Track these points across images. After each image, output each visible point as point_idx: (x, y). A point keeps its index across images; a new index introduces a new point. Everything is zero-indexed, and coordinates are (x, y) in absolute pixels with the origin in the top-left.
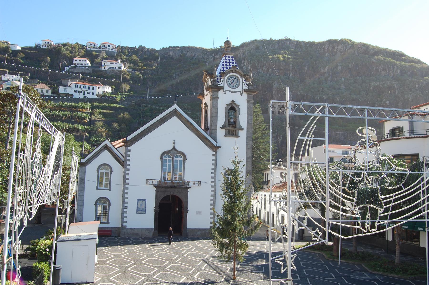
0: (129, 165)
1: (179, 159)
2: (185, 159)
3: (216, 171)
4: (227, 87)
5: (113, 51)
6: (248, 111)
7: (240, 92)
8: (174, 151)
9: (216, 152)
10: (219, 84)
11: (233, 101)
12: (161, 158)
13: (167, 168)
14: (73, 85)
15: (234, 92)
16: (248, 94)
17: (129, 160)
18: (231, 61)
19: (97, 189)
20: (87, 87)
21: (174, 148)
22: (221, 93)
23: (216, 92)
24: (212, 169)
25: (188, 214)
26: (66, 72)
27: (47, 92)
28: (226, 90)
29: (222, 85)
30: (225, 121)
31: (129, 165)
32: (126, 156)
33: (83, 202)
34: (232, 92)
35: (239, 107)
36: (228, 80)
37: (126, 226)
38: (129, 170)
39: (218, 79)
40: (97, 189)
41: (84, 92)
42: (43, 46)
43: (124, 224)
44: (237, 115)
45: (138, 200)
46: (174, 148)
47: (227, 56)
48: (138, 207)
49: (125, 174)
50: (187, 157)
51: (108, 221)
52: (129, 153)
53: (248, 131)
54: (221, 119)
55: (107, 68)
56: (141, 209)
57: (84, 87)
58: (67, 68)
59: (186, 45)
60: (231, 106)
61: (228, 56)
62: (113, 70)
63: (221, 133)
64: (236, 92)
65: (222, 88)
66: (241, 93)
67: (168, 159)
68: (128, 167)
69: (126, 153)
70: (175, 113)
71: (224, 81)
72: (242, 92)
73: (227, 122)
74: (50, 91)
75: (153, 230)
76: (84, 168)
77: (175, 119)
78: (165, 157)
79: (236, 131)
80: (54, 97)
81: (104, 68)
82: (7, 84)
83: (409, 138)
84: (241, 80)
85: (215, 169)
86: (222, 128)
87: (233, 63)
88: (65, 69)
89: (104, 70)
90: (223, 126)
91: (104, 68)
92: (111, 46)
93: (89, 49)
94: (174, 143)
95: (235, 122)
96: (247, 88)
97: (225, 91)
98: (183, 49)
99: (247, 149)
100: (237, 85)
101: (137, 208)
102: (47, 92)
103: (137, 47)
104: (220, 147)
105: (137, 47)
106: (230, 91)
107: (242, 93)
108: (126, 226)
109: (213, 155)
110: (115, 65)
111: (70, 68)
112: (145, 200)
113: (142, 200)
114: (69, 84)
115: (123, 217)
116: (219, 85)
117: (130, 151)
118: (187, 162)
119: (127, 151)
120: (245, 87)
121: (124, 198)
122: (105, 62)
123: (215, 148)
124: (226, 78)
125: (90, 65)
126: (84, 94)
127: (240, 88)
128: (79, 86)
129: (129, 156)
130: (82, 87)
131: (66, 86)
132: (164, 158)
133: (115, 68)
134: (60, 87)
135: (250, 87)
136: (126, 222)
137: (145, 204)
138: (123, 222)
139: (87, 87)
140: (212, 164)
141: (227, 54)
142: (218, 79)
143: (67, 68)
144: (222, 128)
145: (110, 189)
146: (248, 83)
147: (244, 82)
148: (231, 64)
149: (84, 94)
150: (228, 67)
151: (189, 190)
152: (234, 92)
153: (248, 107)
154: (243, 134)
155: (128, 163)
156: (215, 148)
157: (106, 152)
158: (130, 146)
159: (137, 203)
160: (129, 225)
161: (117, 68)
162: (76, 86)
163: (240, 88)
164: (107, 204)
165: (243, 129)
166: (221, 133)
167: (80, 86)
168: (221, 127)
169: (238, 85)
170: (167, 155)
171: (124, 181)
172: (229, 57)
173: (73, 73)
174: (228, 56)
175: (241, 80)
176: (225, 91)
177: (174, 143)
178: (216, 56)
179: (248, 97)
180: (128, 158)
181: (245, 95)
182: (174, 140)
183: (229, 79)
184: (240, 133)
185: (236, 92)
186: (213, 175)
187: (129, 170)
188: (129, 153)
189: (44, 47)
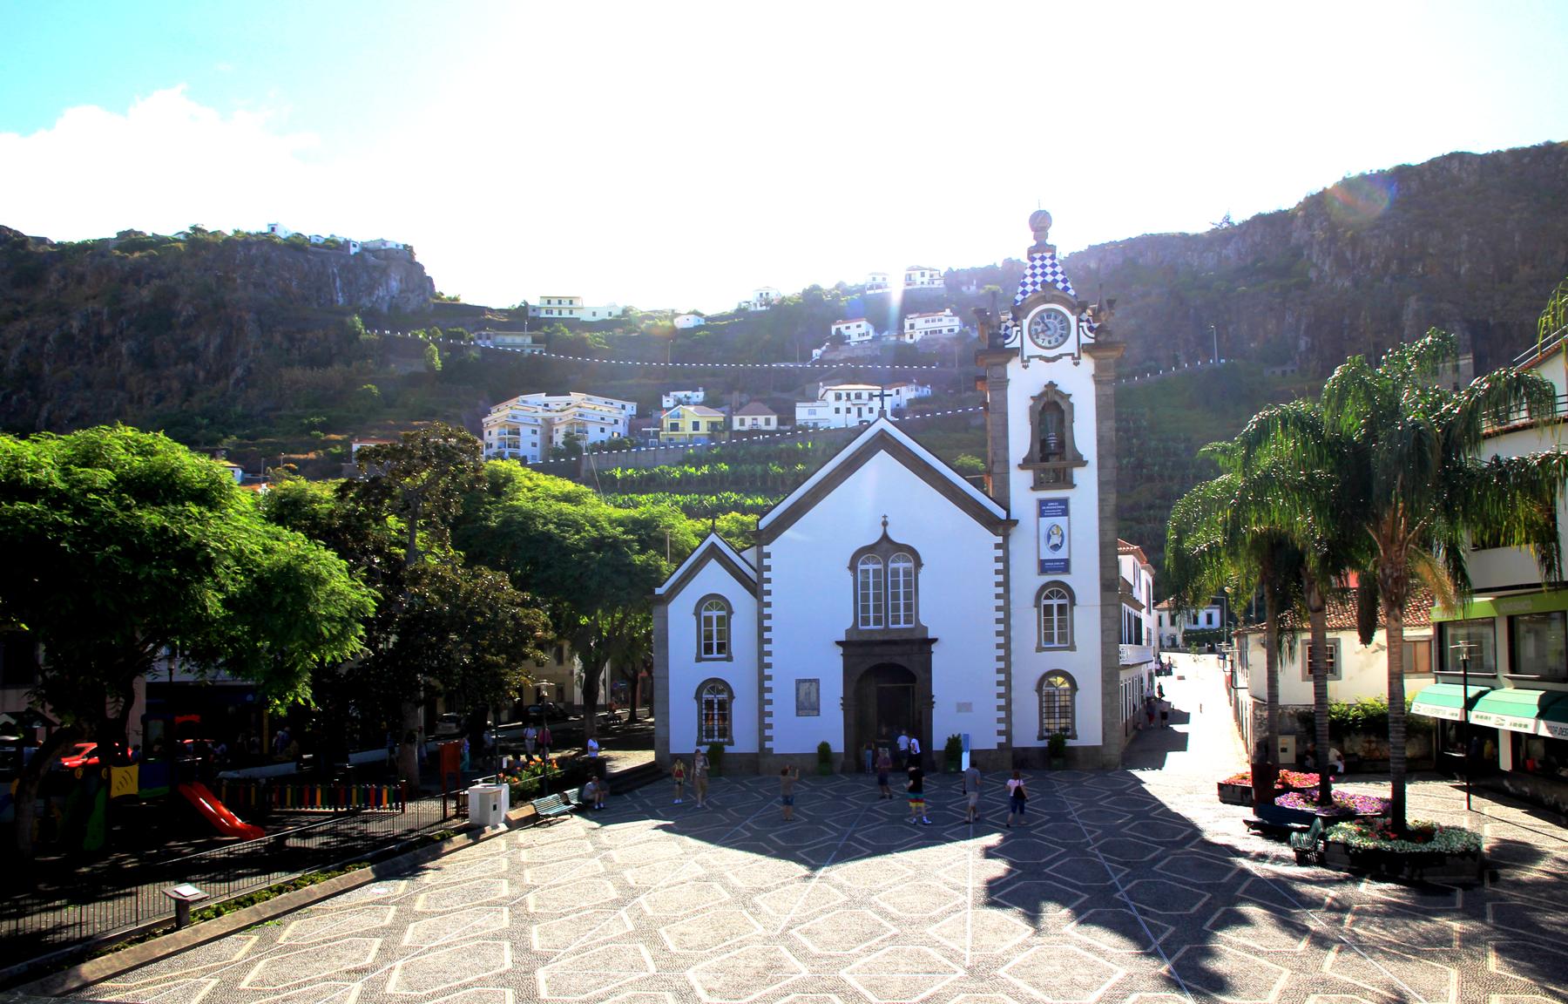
0: (769, 593)
1: (901, 566)
2: (918, 564)
3: (1007, 590)
4: (1030, 349)
5: (932, 286)
6: (1098, 408)
7: (1072, 354)
8: (885, 545)
9: (1006, 537)
10: (1007, 341)
11: (1051, 386)
12: (853, 567)
13: (871, 591)
14: (831, 396)
15: (1054, 359)
16: (1094, 358)
17: (769, 581)
18: (1049, 270)
19: (699, 659)
20: (865, 396)
21: (885, 537)
22: (1013, 368)
23: (999, 367)
24: (998, 584)
25: (936, 714)
26: (813, 364)
27: (768, 422)
28: (1029, 357)
29: (1017, 344)
30: (1032, 445)
31: (769, 593)
32: (760, 569)
33: (668, 694)
34: (1048, 360)
35: (1072, 400)
36: (1033, 327)
37: (771, 749)
38: (769, 605)
39: (1007, 328)
40: (699, 659)
41: (860, 410)
42: (755, 305)
43: (768, 745)
44: (1067, 423)
45: (799, 682)
46: (885, 537)
47: (1037, 255)
48: (801, 698)
49: (762, 617)
50: (924, 561)
51: (731, 737)
52: (766, 562)
53: (1101, 467)
54: (1020, 440)
55: (918, 336)
56: (806, 704)
57: (858, 396)
58: (817, 353)
59: (1135, 232)
60: (1045, 399)
61: (1039, 255)
62: (933, 340)
63: (1020, 483)
64: (1060, 356)
65: (1016, 352)
66: (1073, 358)
67: (871, 567)
68: (766, 599)
69: (760, 561)
70: (884, 441)
71: (1021, 331)
72: (1076, 355)
73: (1038, 447)
74: (774, 419)
75: (843, 758)
76: (662, 608)
77: (882, 457)
78: (863, 563)
79: (1065, 469)
80: (783, 433)
81: (911, 337)
82: (672, 416)
83: (1497, 434)
84: (1073, 319)
85: (1006, 584)
86: (1021, 467)
87: (1054, 274)
88: (814, 355)
89: (911, 341)
90: (1025, 460)
91: (911, 337)
92: (927, 273)
93: (871, 292)
94: (885, 524)
95: (1061, 444)
96: (1092, 341)
97: (1025, 358)
98: (1131, 243)
99: (1102, 519)
100: (1061, 336)
101: (797, 700)
102: (768, 422)
103: (999, 265)
104: (1016, 522)
105: (999, 265)
106: (1041, 358)
107: (1079, 358)
108: (771, 749)
109: (998, 546)
110: (939, 324)
111: (824, 352)
112: (817, 681)
113: (810, 680)
114: (821, 391)
115: (763, 726)
116: (1007, 346)
117: (768, 555)
118: (923, 571)
119: (763, 556)
120: (1084, 340)
121: (762, 678)
122: (912, 321)
123: (1002, 526)
124: (1026, 322)
125: (872, 333)
126: (860, 415)
127: (1070, 346)
128: (844, 397)
129: (768, 568)
130: (853, 396)
131: (814, 400)
132: (861, 567)
133: (940, 331)
134: (798, 404)
135: (1102, 338)
136: (770, 738)
137: (818, 690)
138: (763, 739)
139: (865, 396)
140: (997, 572)
141: (1037, 252)
142: (1007, 328)
143: (817, 353)
144: (1021, 467)
145: (729, 658)
146: (1096, 325)
147: (1081, 324)
148: (1039, 279)
149: (860, 415)
150: (1029, 288)
151: (934, 647)
152: (1054, 359)
153: (1097, 396)
154: (1087, 480)
155: (766, 587)
156: (1002, 526)
157: (713, 564)
158: (767, 544)
159: (797, 690)
160: (779, 746)
161: (945, 331)
162: (838, 397)
163: (1070, 346)
164: (724, 696)
165: (1087, 462)
166: (1020, 483)
167: (848, 395)
168: (1019, 465)
169: (1065, 337)
170: (868, 558)
171: (760, 636)
172: (1043, 258)
173: (832, 362)
174: (1039, 255)
175: (1073, 319)
176: (1025, 358)
177: (885, 524)
178: (1224, 251)
179: (1097, 367)
180: (766, 575)
181: (1088, 364)
182: (885, 517)
183: (1038, 324)
184: (1079, 474)
185: (1060, 356)
186: (1001, 602)
187: (769, 605)
188: (766, 562)
189: (759, 308)
